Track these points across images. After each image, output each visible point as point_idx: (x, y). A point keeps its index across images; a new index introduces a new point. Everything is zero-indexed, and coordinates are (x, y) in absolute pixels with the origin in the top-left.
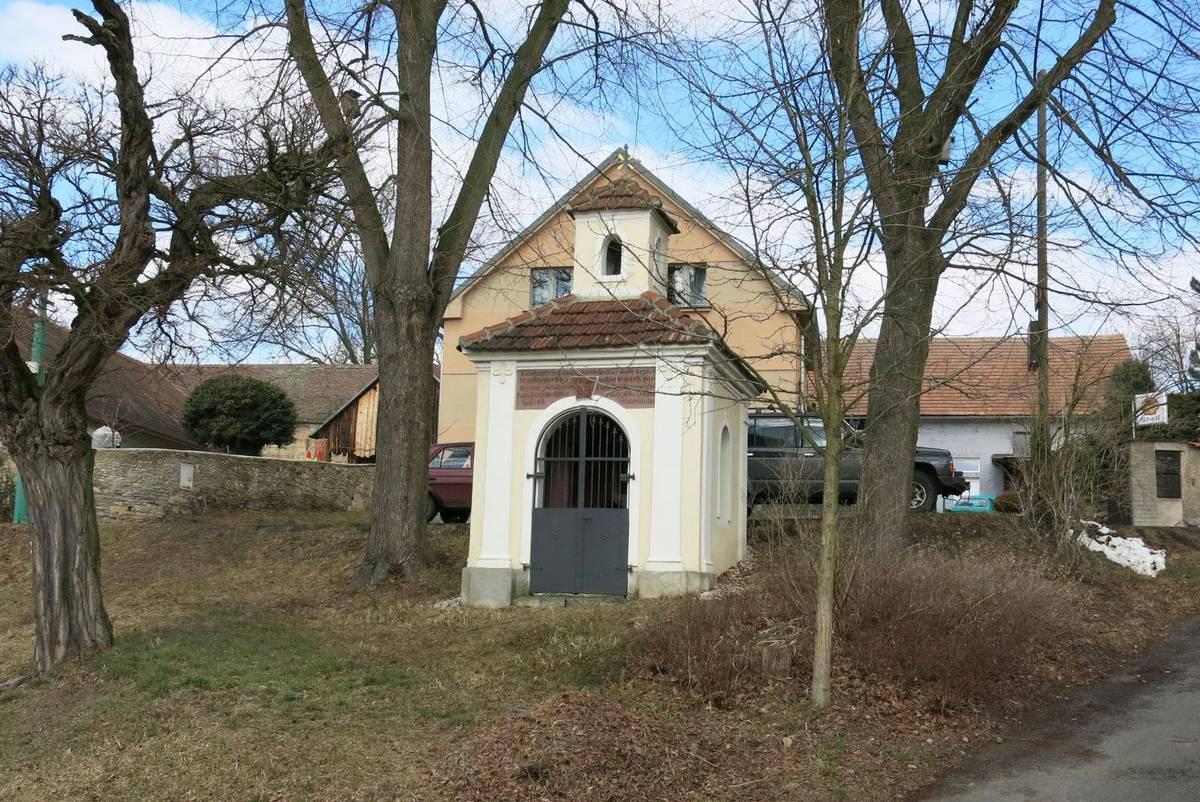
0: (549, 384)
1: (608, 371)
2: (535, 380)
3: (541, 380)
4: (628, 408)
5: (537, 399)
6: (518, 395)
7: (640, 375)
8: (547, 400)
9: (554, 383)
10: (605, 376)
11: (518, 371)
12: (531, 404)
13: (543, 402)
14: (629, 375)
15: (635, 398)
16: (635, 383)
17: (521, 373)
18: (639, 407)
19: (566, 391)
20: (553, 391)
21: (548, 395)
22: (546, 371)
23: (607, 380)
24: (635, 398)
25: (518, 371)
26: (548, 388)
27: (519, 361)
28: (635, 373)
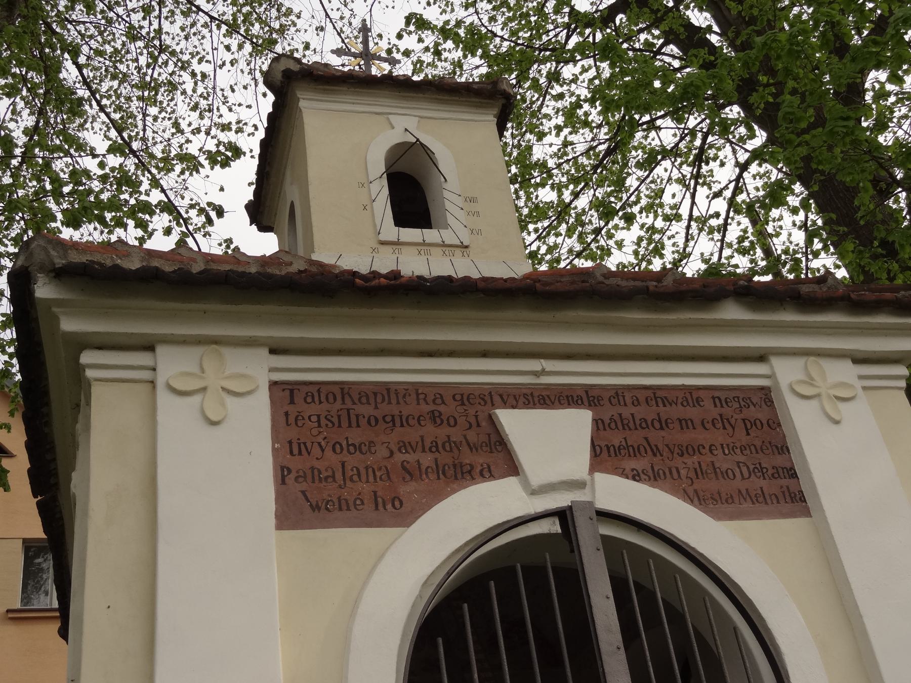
0: (412, 434)
1: (618, 394)
2: (353, 421)
3: (372, 422)
4: (718, 516)
5: (365, 488)
6: (282, 474)
7: (727, 411)
8: (406, 489)
9: (430, 431)
10: (608, 412)
11: (273, 385)
12: (343, 505)
13: (397, 501)
14: (692, 413)
15: (738, 483)
16: (718, 436)
17: (285, 394)
18: (758, 516)
19: (480, 459)
20: (427, 460)
21: (410, 473)
22: (386, 391)
23: (621, 423)
24: (738, 483)
25: (273, 385)
26: (404, 446)
27: (273, 351)
28: (708, 404)
